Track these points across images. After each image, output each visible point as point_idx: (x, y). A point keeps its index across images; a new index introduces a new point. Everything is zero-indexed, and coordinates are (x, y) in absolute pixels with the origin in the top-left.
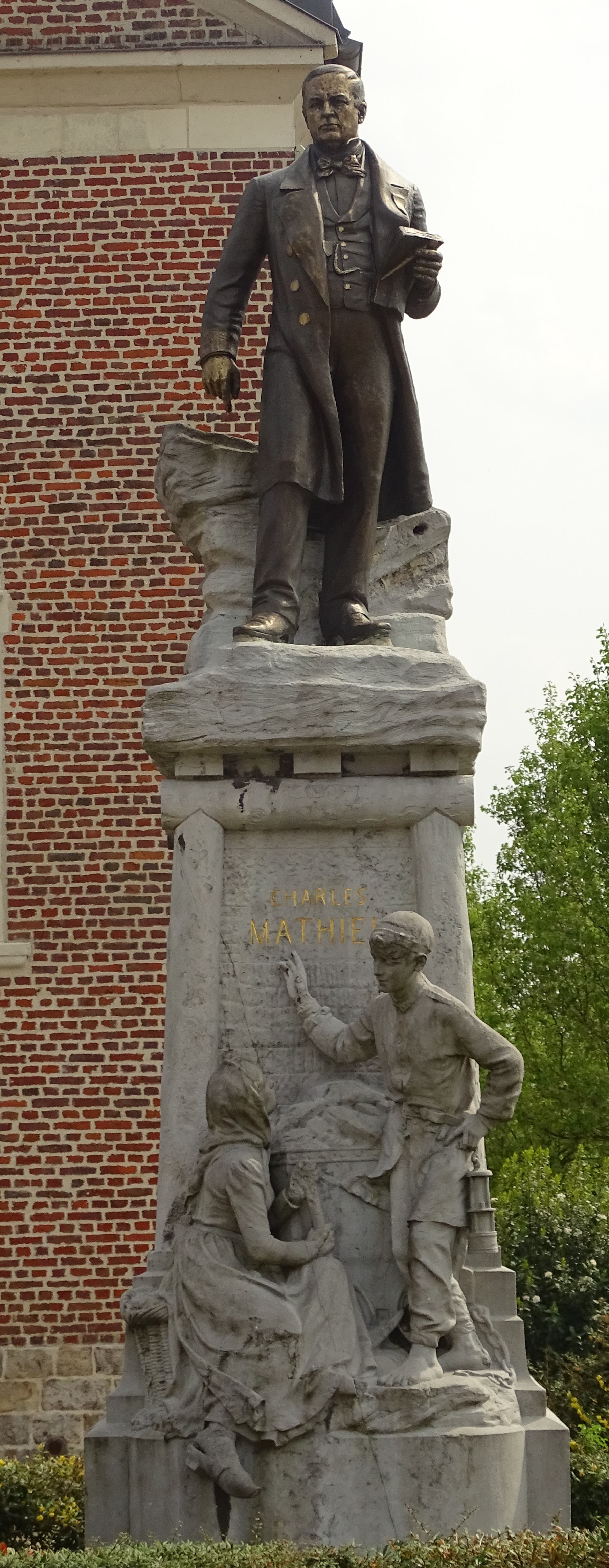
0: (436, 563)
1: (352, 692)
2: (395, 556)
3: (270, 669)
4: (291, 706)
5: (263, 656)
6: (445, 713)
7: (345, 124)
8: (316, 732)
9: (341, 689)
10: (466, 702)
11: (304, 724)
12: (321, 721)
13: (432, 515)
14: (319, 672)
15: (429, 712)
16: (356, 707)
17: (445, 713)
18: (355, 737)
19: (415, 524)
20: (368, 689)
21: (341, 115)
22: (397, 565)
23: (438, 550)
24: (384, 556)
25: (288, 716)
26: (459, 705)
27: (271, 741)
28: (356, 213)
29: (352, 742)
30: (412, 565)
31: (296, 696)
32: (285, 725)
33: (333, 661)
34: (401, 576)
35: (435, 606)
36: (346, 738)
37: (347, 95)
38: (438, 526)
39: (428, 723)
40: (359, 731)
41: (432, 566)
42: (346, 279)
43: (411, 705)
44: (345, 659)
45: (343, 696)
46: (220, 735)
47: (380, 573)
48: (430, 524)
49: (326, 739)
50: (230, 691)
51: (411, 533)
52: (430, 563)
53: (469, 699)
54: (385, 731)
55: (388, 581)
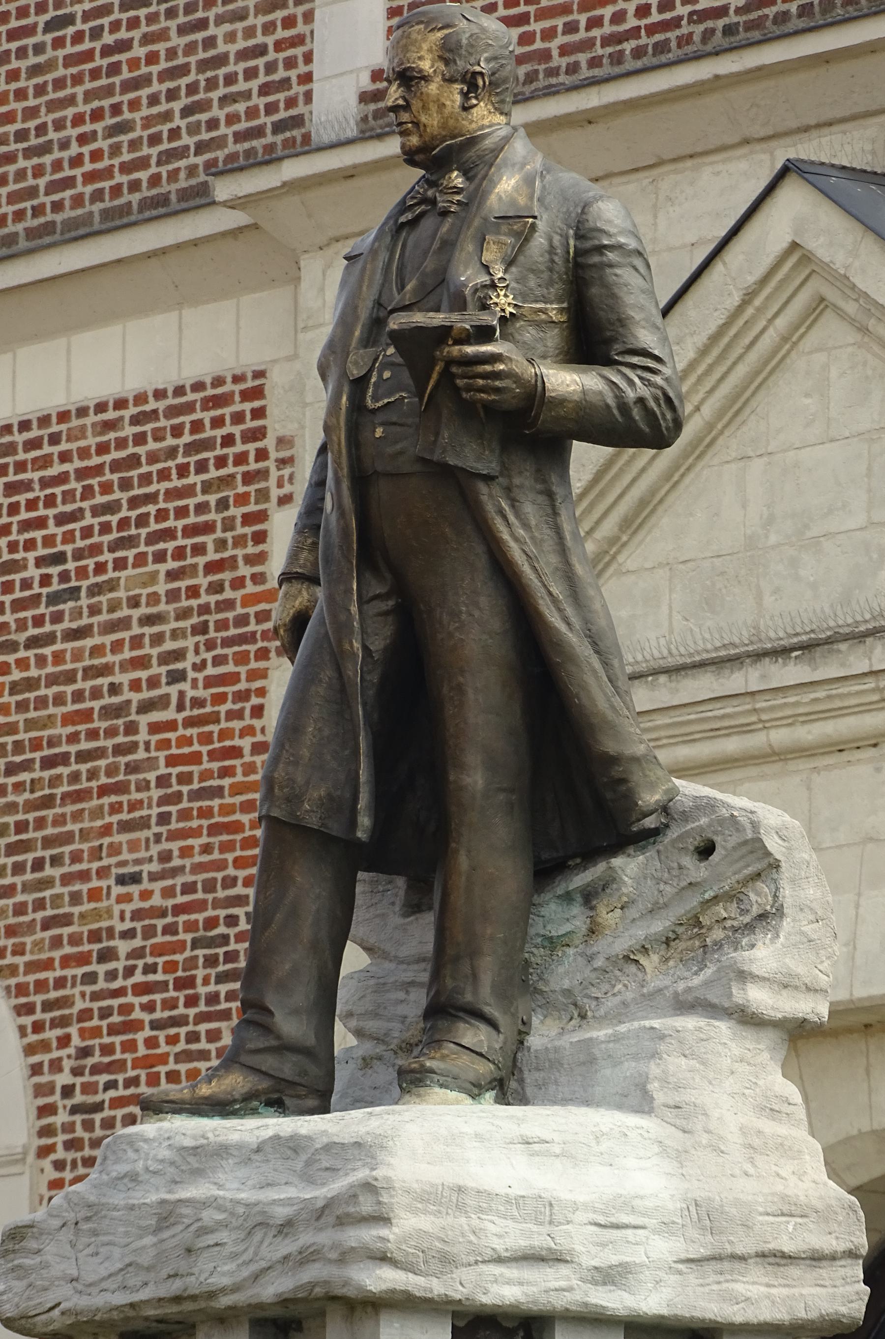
0: (755, 911)
1: (220, 1209)
2: (653, 911)
3: (137, 1174)
4: (149, 1240)
5: (137, 1151)
6: (324, 1238)
7: (423, 119)
8: (175, 1287)
9: (205, 1204)
10: (348, 1215)
11: (164, 1273)
12: (182, 1266)
13: (721, 821)
14: (197, 1173)
15: (306, 1238)
16: (223, 1236)
17: (324, 1238)
18: (223, 1291)
19: (692, 843)
20: (238, 1202)
21: (416, 104)
22: (659, 926)
23: (759, 885)
24: (632, 913)
25: (145, 1259)
26: (343, 1221)
27: (132, 1305)
28: (422, 284)
29: (225, 1301)
30: (705, 920)
31: (153, 1222)
32: (142, 1277)
33: (222, 1151)
34: (681, 945)
35: (715, 1001)
36: (212, 1295)
37: (426, 65)
38: (733, 841)
39: (307, 1256)
40: (226, 1281)
41: (747, 919)
42: (380, 417)
43: (286, 1227)
44: (240, 1146)
45: (209, 1216)
46: (83, 1302)
47: (620, 946)
48: (718, 839)
49: (193, 1298)
50: (88, 1219)
51: (688, 861)
52: (744, 912)
53: (351, 1209)
54: (256, 1277)
55: (655, 958)
